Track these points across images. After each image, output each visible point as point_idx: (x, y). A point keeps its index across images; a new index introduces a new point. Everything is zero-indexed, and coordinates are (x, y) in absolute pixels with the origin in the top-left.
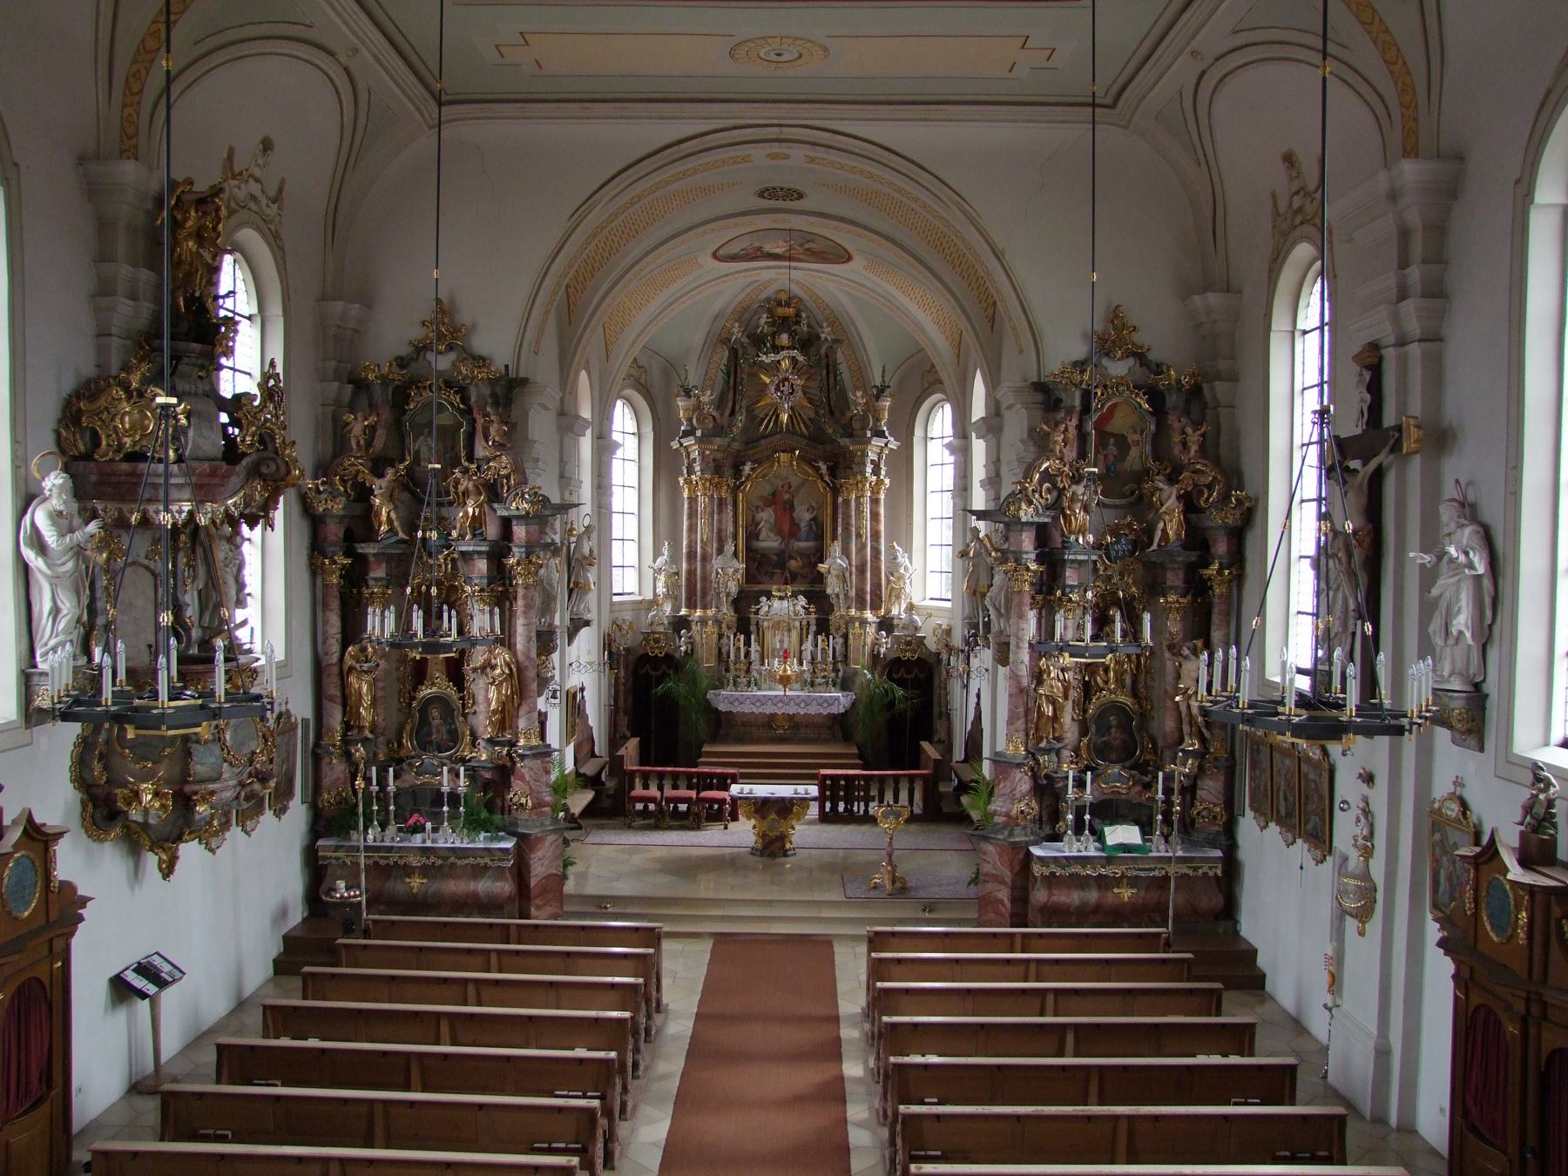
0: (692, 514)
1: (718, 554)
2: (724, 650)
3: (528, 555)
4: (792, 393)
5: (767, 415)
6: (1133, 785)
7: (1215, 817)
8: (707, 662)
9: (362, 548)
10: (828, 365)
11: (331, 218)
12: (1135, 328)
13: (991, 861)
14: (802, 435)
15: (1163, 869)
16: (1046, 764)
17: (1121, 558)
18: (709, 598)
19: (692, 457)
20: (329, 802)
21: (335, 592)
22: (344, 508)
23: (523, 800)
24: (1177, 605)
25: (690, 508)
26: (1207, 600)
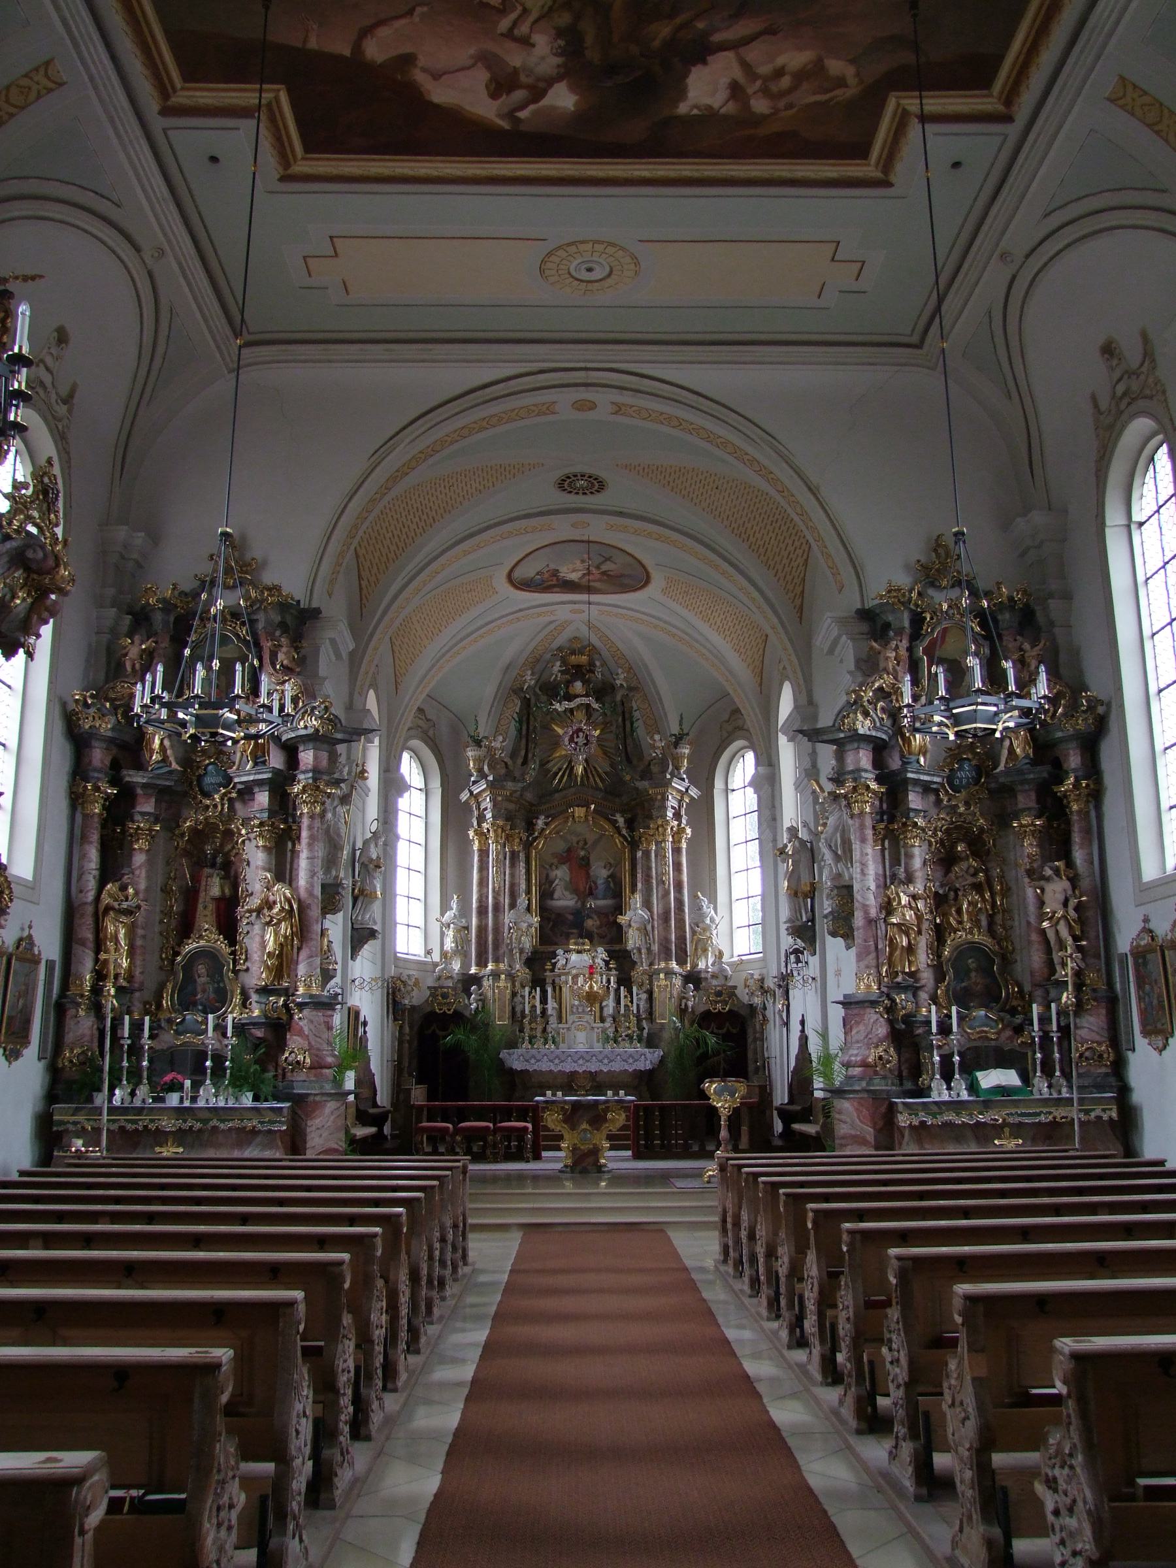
0: (483, 868)
1: (510, 910)
2: (518, 1009)
3: (315, 779)
4: (586, 744)
5: (560, 769)
6: (1003, 1029)
7: (1101, 1056)
8: (501, 1021)
9: (129, 775)
10: (623, 712)
11: (121, 451)
13: (848, 1120)
14: (597, 788)
15: (1050, 1113)
16: (904, 1003)
17: (967, 787)
18: (501, 951)
19: (482, 808)
20: (71, 1061)
21: (96, 823)
22: (113, 729)
23: (300, 1058)
24: (1032, 828)
25: (481, 861)
26: (1063, 826)
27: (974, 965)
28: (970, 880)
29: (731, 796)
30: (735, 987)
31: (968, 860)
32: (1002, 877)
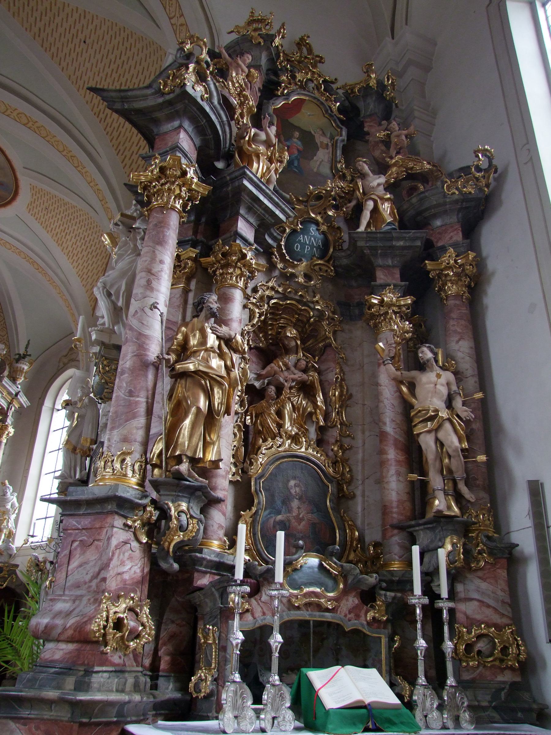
7: (504, 650)
12: (321, 58)
16: (184, 518)
27: (298, 489)
28: (299, 375)
29: (56, 414)
30: (17, 566)
31: (297, 353)
32: (341, 383)
